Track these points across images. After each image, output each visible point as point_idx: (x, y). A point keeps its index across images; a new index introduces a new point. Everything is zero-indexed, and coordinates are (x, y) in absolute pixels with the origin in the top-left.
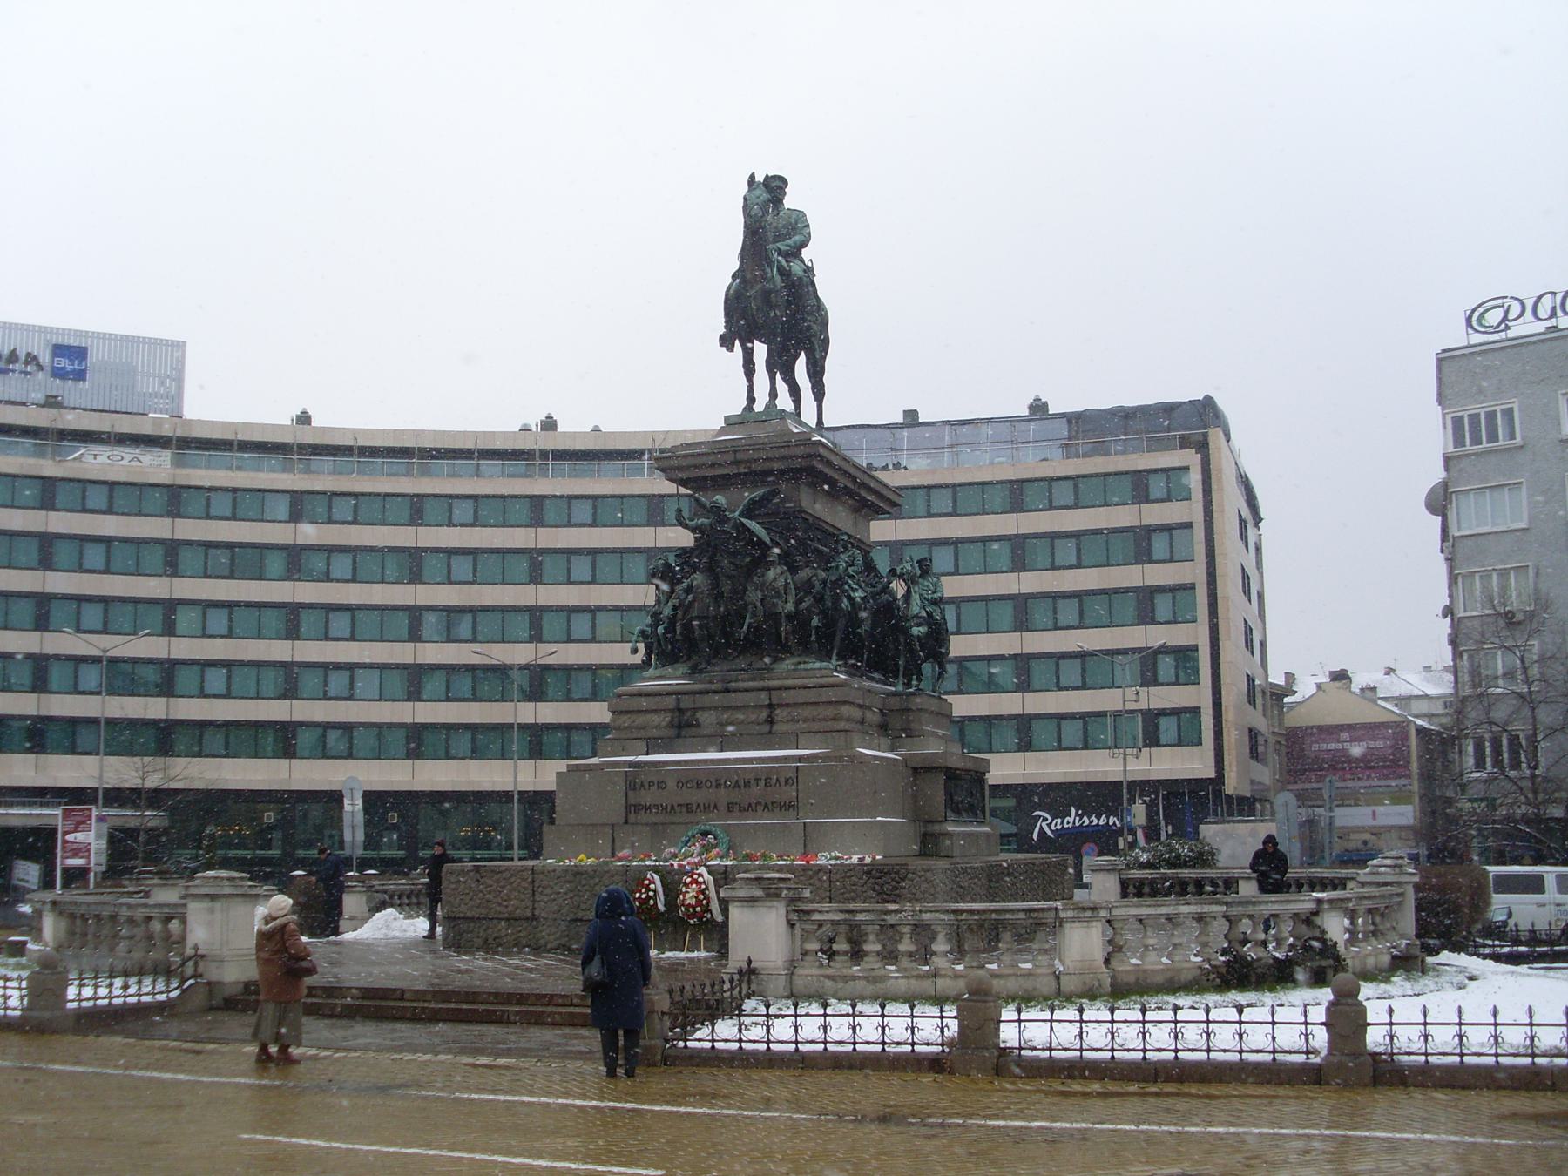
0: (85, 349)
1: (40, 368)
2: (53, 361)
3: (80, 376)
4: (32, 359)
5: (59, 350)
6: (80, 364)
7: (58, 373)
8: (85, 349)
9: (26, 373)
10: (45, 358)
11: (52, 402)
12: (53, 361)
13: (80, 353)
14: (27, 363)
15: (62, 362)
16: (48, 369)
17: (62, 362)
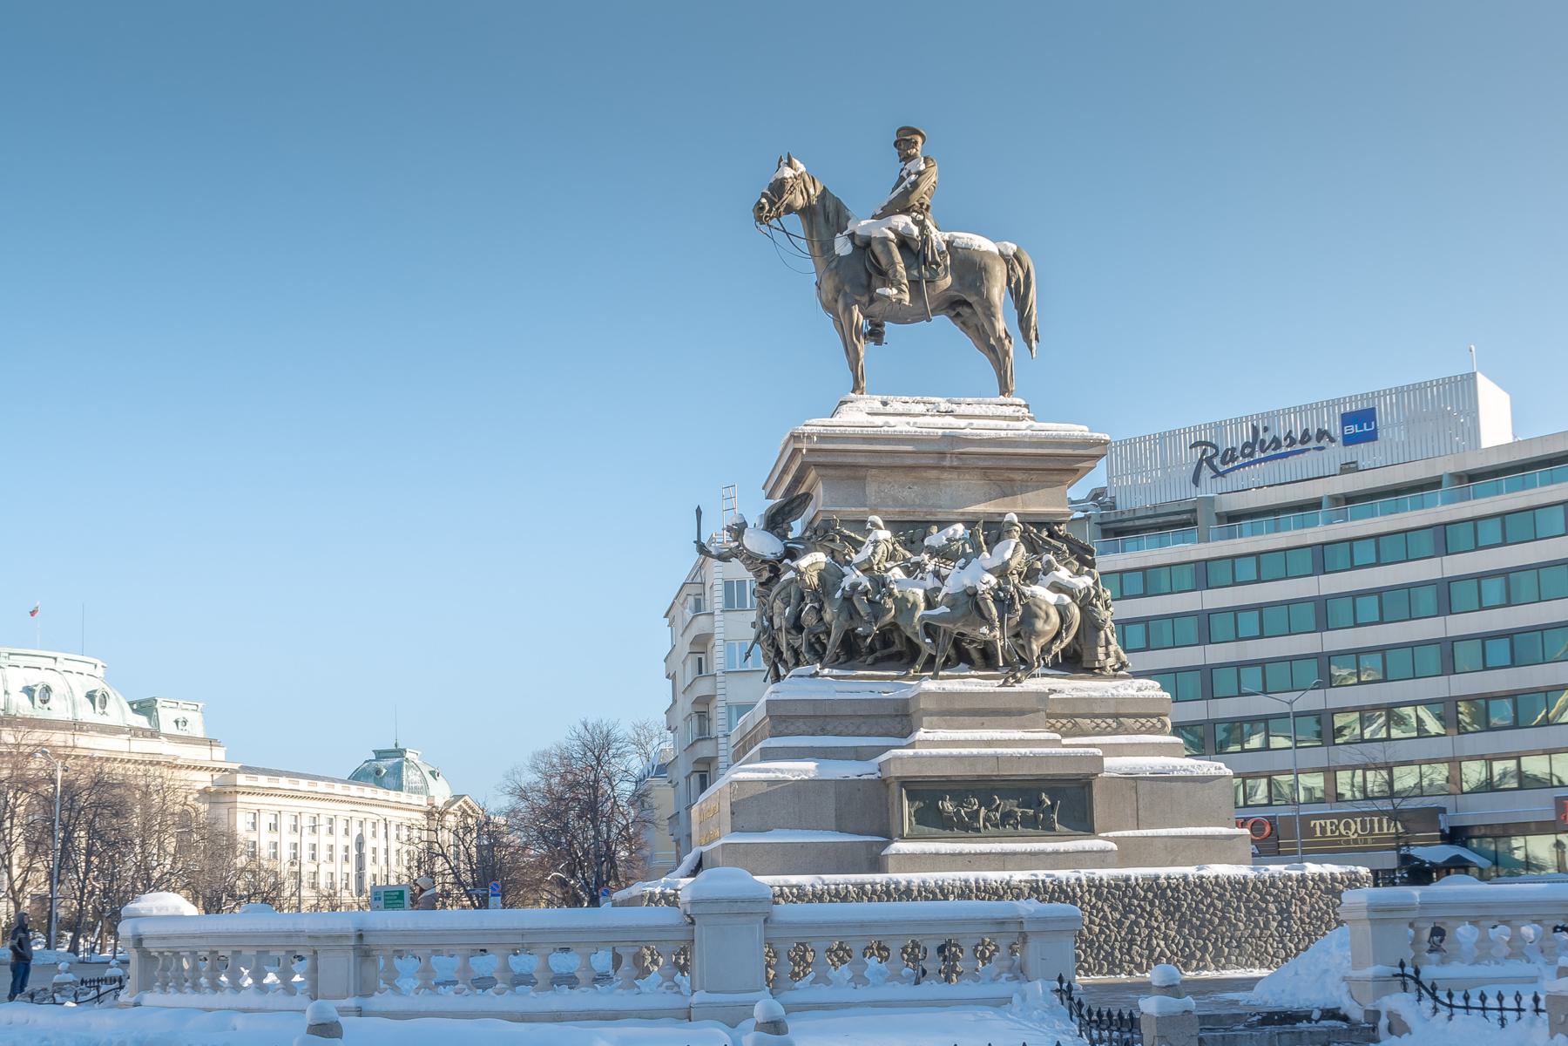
0: (1373, 409)
1: (1332, 440)
2: (1343, 429)
3: (1371, 437)
4: (1322, 434)
5: (1347, 419)
6: (1369, 426)
7: (1349, 440)
8: (1373, 409)
9: (1321, 449)
10: (1336, 429)
11: (1349, 468)
12: (1343, 429)
13: (1367, 416)
14: (1319, 439)
15: (1353, 429)
16: (1340, 439)
17: (1353, 429)
